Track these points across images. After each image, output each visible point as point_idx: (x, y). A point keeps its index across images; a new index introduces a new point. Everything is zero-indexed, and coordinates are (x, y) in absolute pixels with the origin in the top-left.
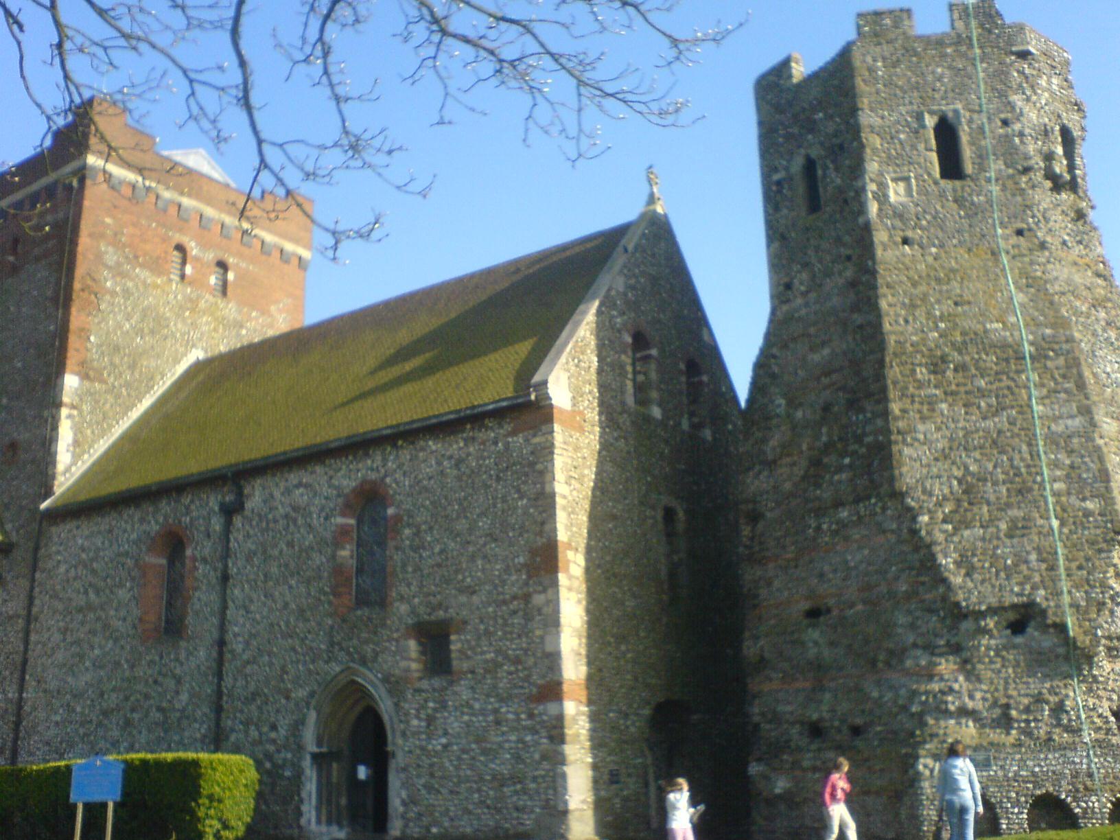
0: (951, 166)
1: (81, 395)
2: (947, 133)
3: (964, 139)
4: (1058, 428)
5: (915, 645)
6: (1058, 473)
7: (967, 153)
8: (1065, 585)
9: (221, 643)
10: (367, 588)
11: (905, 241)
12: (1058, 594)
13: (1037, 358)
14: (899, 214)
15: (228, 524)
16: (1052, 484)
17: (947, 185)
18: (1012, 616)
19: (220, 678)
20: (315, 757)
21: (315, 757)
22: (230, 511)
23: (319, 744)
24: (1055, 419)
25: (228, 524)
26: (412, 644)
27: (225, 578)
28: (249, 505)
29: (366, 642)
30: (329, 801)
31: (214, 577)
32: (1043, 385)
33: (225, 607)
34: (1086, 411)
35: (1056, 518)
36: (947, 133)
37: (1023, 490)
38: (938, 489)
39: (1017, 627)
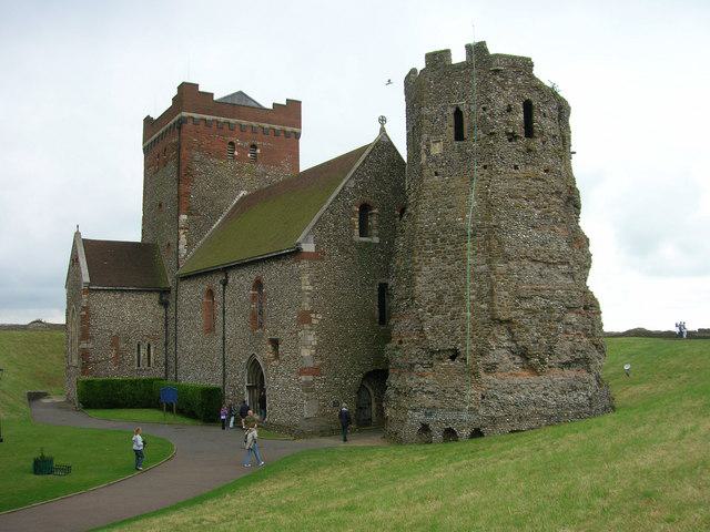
0: (459, 136)
1: (189, 223)
2: (458, 114)
3: (465, 119)
7: (466, 126)
8: (468, 342)
9: (224, 338)
10: (257, 319)
11: (436, 174)
13: (473, 235)
16: (470, 295)
17: (456, 144)
22: (225, 283)
26: (270, 346)
27: (224, 312)
36: (458, 114)
37: (460, 298)
39: (453, 358)
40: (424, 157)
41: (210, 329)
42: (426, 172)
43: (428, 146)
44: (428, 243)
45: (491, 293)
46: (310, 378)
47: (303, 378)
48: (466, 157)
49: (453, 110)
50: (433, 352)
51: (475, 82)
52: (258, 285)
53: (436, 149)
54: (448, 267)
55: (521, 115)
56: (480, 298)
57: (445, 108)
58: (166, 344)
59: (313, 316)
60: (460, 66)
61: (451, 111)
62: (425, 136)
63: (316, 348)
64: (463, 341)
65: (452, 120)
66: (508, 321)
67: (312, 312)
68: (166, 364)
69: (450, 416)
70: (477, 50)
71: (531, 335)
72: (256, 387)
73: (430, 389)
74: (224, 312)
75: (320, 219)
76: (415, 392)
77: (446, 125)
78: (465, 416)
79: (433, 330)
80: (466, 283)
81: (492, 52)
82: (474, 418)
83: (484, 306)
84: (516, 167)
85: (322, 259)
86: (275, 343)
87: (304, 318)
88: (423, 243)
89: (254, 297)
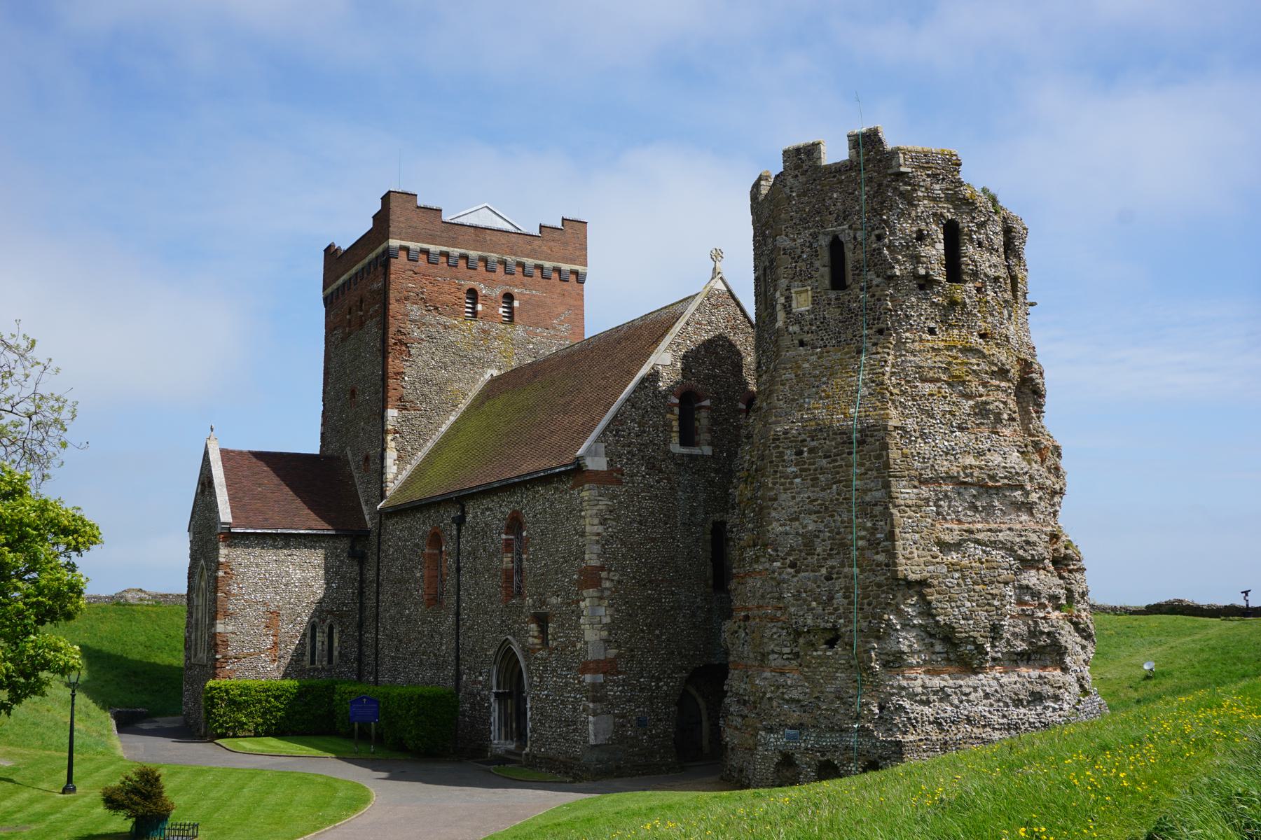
0: (838, 282)
4: (868, 499)
5: (773, 652)
6: (863, 533)
8: (855, 616)
9: (458, 614)
11: (802, 344)
12: (851, 622)
13: (861, 443)
14: (799, 320)
15: (459, 531)
17: (833, 294)
18: (829, 636)
19: (458, 639)
20: (497, 695)
21: (497, 695)
22: (460, 521)
23: (498, 687)
24: (866, 491)
25: (459, 531)
26: (533, 626)
27: (458, 569)
28: (468, 519)
29: (515, 622)
30: (506, 726)
31: (454, 566)
32: (863, 465)
33: (459, 590)
34: (887, 486)
35: (858, 566)
37: (841, 546)
38: (791, 541)
39: (831, 643)
40: (781, 316)
41: (435, 600)
42: (785, 341)
43: (788, 299)
44: (789, 455)
45: (891, 536)
46: (600, 678)
47: (588, 678)
48: (849, 318)
49: (828, 239)
50: (798, 634)
51: (864, 192)
52: (515, 524)
53: (802, 304)
54: (821, 495)
55: (940, 246)
56: (874, 544)
57: (815, 236)
58: (360, 626)
59: (604, 574)
60: (838, 169)
61: (824, 241)
62: (783, 282)
63: (609, 628)
64: (846, 615)
65: (825, 256)
66: (923, 583)
67: (602, 568)
68: (359, 660)
69: (829, 740)
70: (867, 143)
71: (961, 610)
72: (509, 695)
73: (795, 695)
74: (458, 569)
75: (615, 417)
76: (770, 699)
77: (817, 264)
78: (853, 741)
79: (797, 597)
80: (851, 521)
81: (889, 146)
82: (867, 744)
83: (881, 558)
84: (932, 331)
85: (619, 483)
86: (542, 620)
87: (591, 578)
88: (781, 454)
89: (508, 544)
